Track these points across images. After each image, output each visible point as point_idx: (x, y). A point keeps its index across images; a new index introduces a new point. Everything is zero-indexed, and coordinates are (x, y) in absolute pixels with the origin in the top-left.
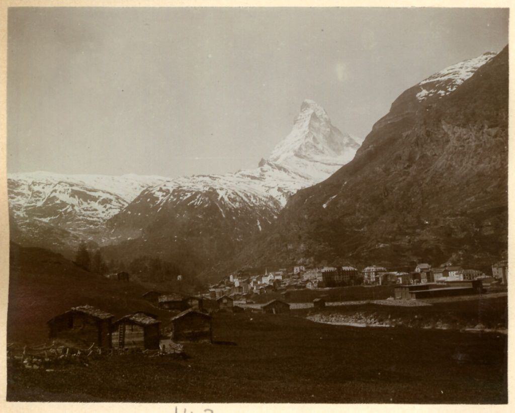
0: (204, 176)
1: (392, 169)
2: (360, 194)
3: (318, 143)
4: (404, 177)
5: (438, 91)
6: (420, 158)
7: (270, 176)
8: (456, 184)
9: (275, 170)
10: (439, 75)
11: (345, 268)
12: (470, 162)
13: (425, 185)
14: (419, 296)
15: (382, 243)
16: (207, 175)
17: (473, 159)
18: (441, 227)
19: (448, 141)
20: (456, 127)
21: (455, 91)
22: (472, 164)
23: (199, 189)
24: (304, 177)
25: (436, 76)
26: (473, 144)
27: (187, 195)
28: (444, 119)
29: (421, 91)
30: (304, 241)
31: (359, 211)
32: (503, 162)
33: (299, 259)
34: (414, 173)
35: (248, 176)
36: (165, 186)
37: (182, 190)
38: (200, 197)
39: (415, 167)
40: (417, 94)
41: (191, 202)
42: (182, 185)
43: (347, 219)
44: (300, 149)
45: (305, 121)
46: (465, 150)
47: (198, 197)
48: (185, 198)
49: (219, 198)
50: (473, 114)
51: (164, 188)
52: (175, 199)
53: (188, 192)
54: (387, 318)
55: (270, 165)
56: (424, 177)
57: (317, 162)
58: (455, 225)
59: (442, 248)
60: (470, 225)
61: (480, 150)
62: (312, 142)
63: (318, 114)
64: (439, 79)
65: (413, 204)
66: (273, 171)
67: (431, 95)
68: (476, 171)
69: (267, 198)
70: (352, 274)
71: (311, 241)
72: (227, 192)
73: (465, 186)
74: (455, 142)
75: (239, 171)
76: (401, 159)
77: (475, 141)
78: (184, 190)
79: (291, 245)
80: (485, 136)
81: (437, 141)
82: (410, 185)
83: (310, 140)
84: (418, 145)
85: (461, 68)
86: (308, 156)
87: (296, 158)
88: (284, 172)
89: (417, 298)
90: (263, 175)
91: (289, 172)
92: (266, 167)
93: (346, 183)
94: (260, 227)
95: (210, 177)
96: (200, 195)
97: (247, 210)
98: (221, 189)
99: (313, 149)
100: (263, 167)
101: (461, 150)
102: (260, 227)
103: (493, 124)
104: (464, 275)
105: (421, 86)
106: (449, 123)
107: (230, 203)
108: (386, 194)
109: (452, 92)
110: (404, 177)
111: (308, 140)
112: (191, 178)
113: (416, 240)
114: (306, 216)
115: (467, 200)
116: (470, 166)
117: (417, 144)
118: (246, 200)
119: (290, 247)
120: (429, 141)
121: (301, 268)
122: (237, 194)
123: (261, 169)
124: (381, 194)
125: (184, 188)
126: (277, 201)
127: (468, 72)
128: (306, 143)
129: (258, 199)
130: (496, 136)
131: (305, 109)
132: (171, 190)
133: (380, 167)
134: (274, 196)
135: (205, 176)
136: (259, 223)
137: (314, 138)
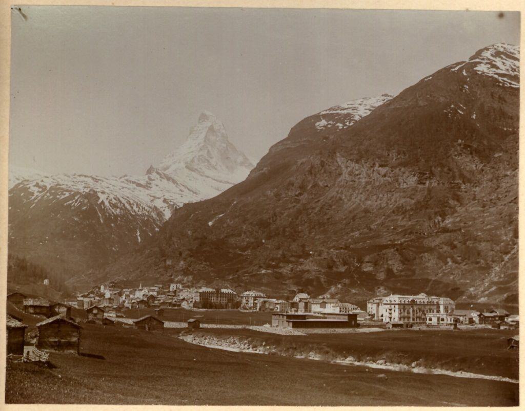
0: (85, 176)
1: (284, 195)
2: (248, 216)
3: (211, 158)
4: (294, 204)
5: (335, 124)
6: (311, 187)
7: (157, 186)
8: (344, 217)
9: (163, 180)
10: (339, 108)
11: (224, 290)
12: (359, 198)
13: (314, 215)
14: (296, 325)
15: (264, 269)
16: (89, 175)
17: (362, 195)
18: (325, 258)
19: (340, 174)
20: (349, 161)
21: (351, 126)
22: (360, 200)
23: (78, 189)
24: (193, 191)
25: (336, 108)
26: (363, 180)
27: (65, 194)
28: (339, 152)
29: (321, 120)
30: (184, 258)
31: (245, 233)
32: (388, 202)
33: (177, 276)
34: (304, 202)
35: (134, 182)
36: (42, 181)
37: (59, 188)
38: (78, 198)
39: (306, 195)
40: (316, 123)
41: (68, 203)
42: (61, 182)
43: (232, 240)
44: (192, 161)
45: (201, 133)
46: (356, 185)
47: (76, 198)
48: (63, 197)
49: (99, 202)
50: (367, 151)
51: (41, 184)
52: (51, 197)
53: (67, 191)
54: (261, 345)
55: (158, 173)
56: (314, 206)
57: (208, 177)
58: (337, 257)
59: (322, 280)
60: (352, 259)
61: (369, 187)
62: (207, 156)
63: (216, 127)
64: (339, 111)
65: (300, 232)
66: (161, 180)
67: (330, 126)
68: (363, 207)
69: (151, 208)
70: (230, 298)
71: (192, 259)
72: (109, 196)
73: (352, 220)
74: (347, 176)
75: (124, 176)
76: (293, 185)
77: (366, 178)
78: (62, 189)
81: (330, 172)
82: (299, 212)
83: (204, 153)
84: (311, 174)
85: (360, 104)
86: (199, 170)
87: (186, 170)
88: (172, 184)
89: (293, 327)
90: (149, 184)
91: (177, 184)
92: (154, 175)
93: (235, 203)
94: (139, 238)
95: (93, 178)
96: (78, 196)
97: (128, 218)
98: (103, 193)
99: (206, 164)
100: (150, 175)
101: (352, 184)
102: (139, 238)
103: (383, 163)
104: (340, 308)
105: (320, 116)
106: (343, 157)
107: (110, 208)
109: (349, 127)
110: (294, 204)
111: (201, 153)
112: (72, 177)
113: (298, 269)
114: (189, 232)
115: (352, 234)
116: (359, 202)
117: (310, 172)
118: (128, 207)
119: (169, 262)
120: (323, 171)
121: (178, 286)
122: (119, 200)
123: (149, 177)
125: (62, 186)
126: (161, 212)
127: (366, 109)
128: (199, 156)
129: (141, 208)
130: (385, 176)
131: (203, 120)
132: (48, 187)
133: (271, 191)
134: (158, 207)
135: (88, 177)
136: (138, 234)
137: (208, 151)
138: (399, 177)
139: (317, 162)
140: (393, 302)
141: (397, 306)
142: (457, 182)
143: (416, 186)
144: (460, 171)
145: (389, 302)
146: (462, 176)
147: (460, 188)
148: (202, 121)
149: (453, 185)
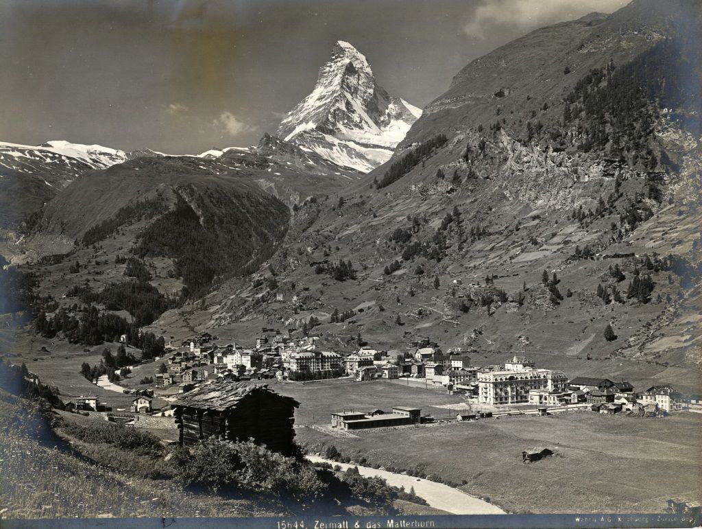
3: (354, 112)
11: (325, 354)
12: (527, 196)
19: (506, 159)
33: (287, 319)
45: (336, 75)
63: (357, 65)
69: (267, 199)
74: (513, 163)
79: (282, 295)
80: (549, 162)
103: (559, 147)
108: (416, 231)
124: (410, 229)
138: (579, 168)
139: (475, 144)
140: (488, 381)
141: (492, 385)
142: (657, 171)
143: (600, 180)
144: (663, 154)
145: (484, 380)
146: (665, 159)
147: (661, 179)
148: (336, 58)
149: (653, 175)
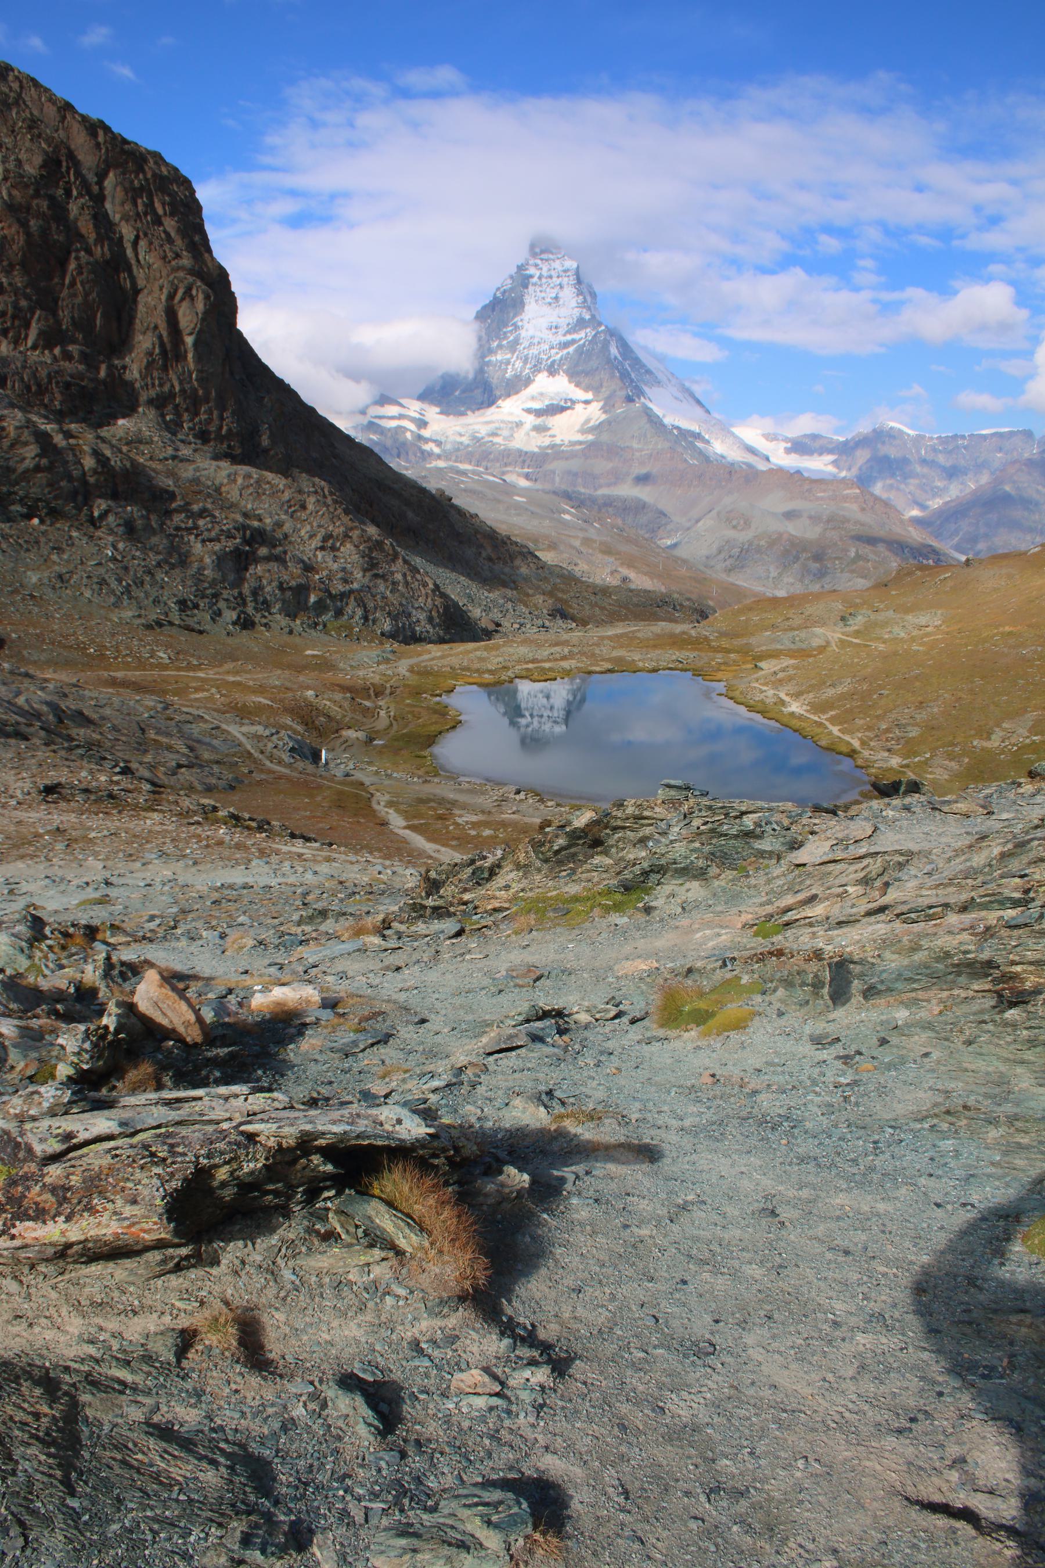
45: (561, 287)
148: (542, 252)
